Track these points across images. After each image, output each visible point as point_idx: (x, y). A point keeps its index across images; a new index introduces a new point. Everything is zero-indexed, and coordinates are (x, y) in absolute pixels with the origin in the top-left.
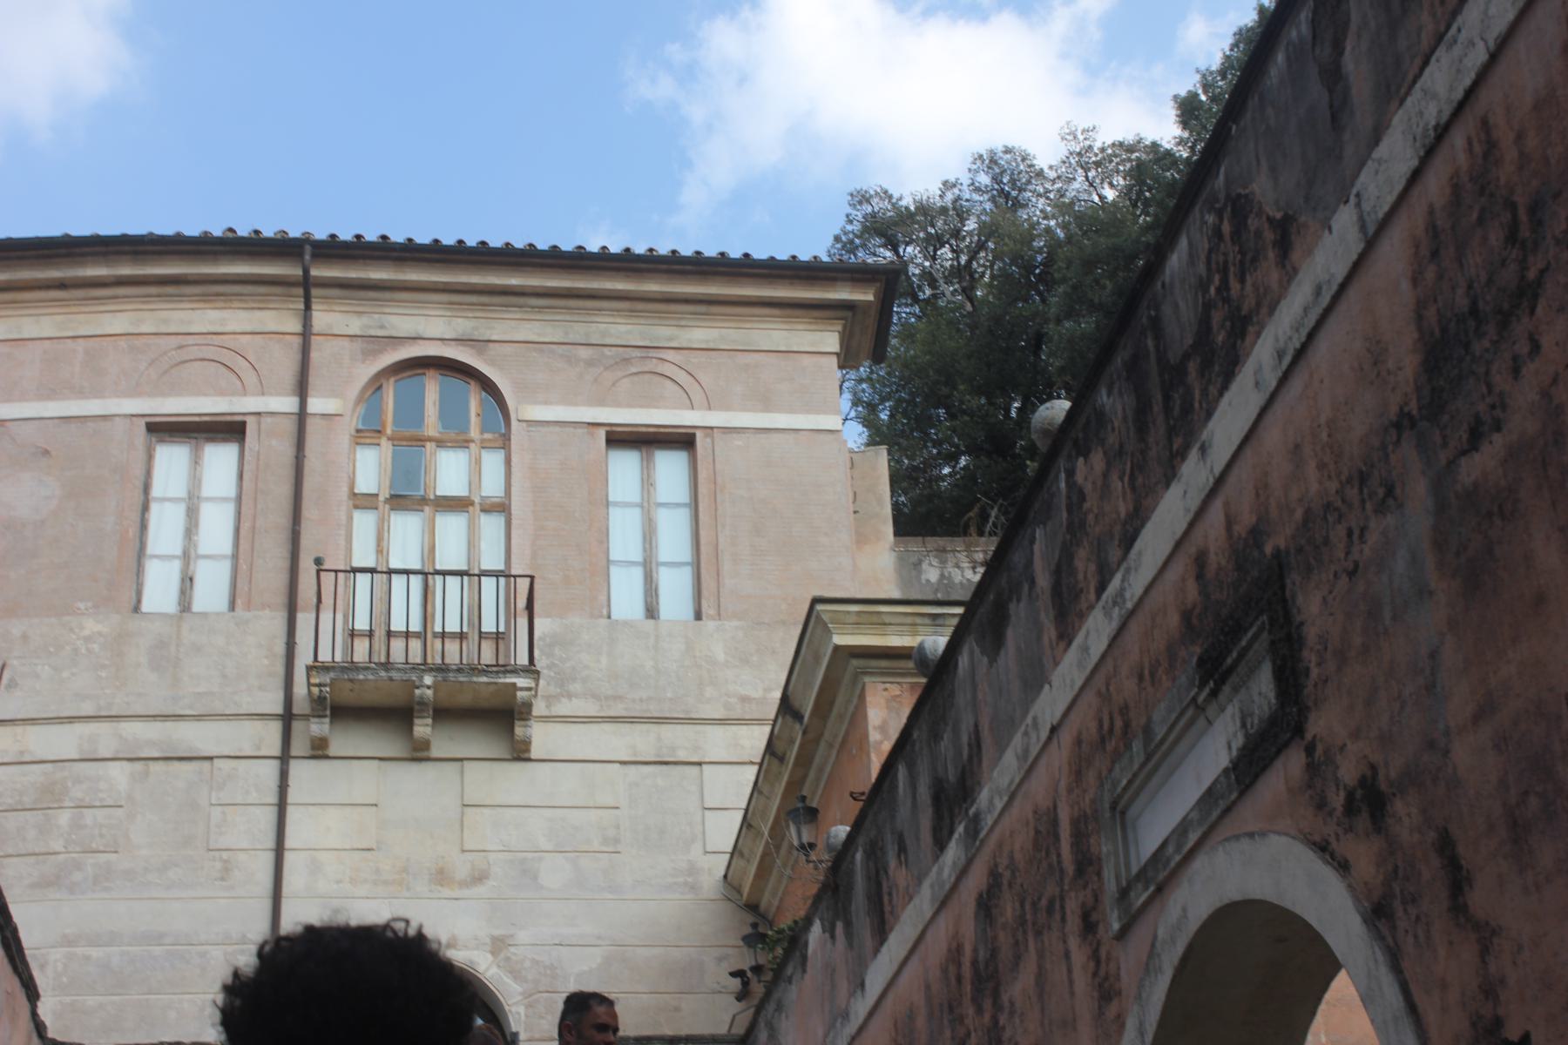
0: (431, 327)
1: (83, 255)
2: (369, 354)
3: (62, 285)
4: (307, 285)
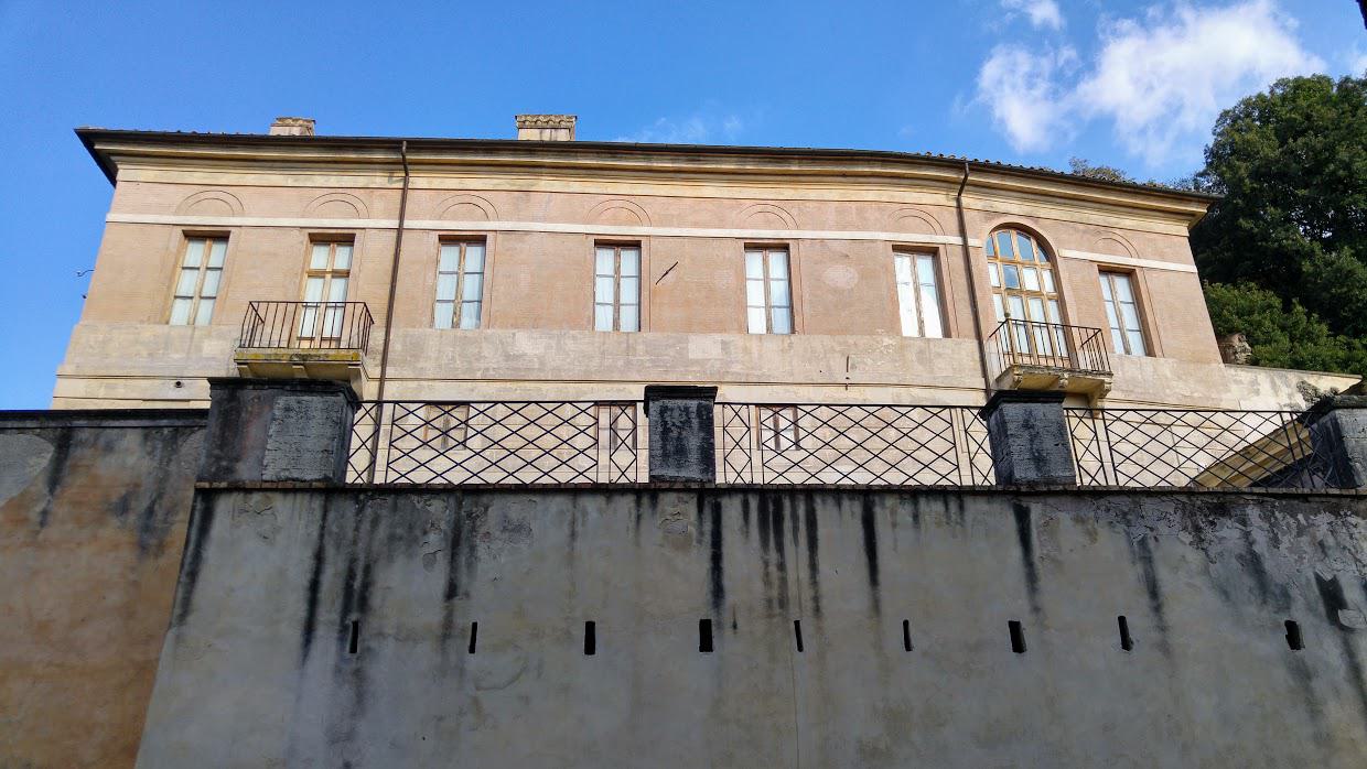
0: (1015, 209)
1: (858, 160)
2: (988, 219)
3: (844, 175)
4: (964, 183)
